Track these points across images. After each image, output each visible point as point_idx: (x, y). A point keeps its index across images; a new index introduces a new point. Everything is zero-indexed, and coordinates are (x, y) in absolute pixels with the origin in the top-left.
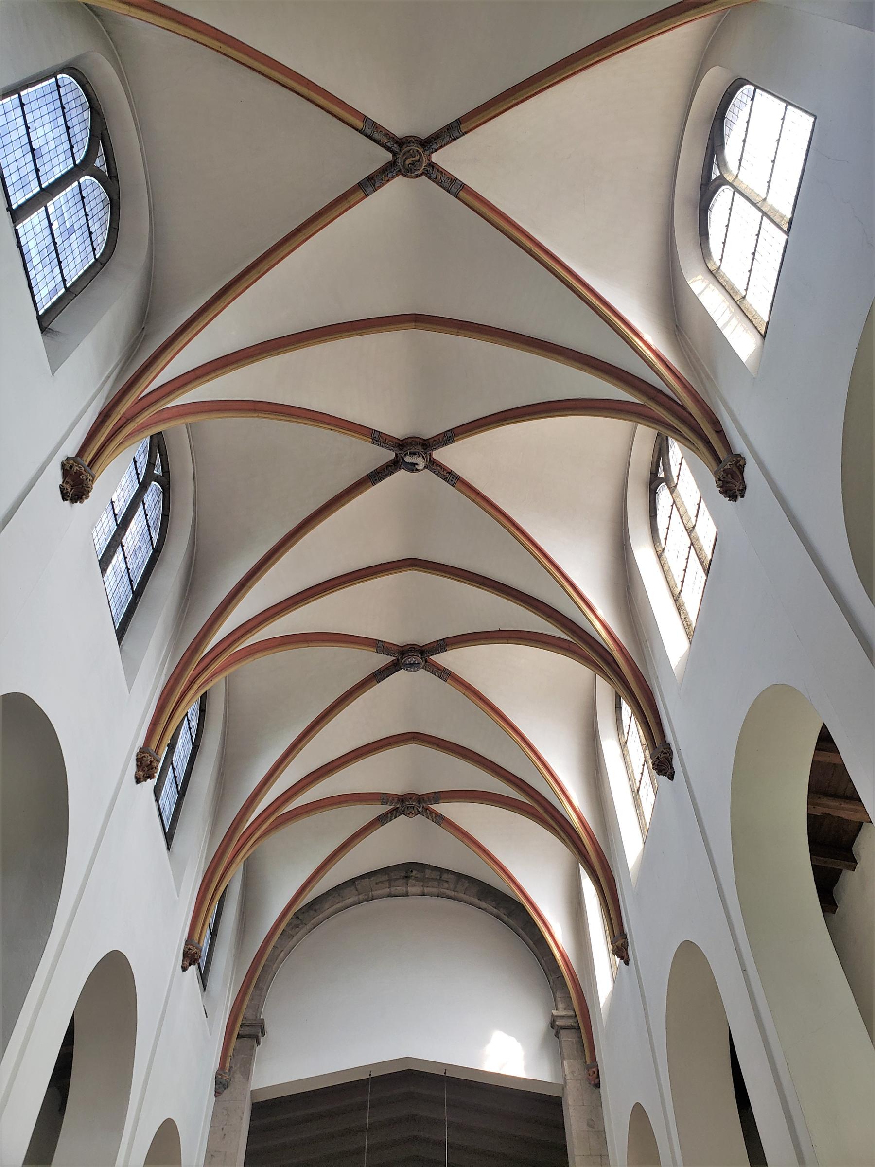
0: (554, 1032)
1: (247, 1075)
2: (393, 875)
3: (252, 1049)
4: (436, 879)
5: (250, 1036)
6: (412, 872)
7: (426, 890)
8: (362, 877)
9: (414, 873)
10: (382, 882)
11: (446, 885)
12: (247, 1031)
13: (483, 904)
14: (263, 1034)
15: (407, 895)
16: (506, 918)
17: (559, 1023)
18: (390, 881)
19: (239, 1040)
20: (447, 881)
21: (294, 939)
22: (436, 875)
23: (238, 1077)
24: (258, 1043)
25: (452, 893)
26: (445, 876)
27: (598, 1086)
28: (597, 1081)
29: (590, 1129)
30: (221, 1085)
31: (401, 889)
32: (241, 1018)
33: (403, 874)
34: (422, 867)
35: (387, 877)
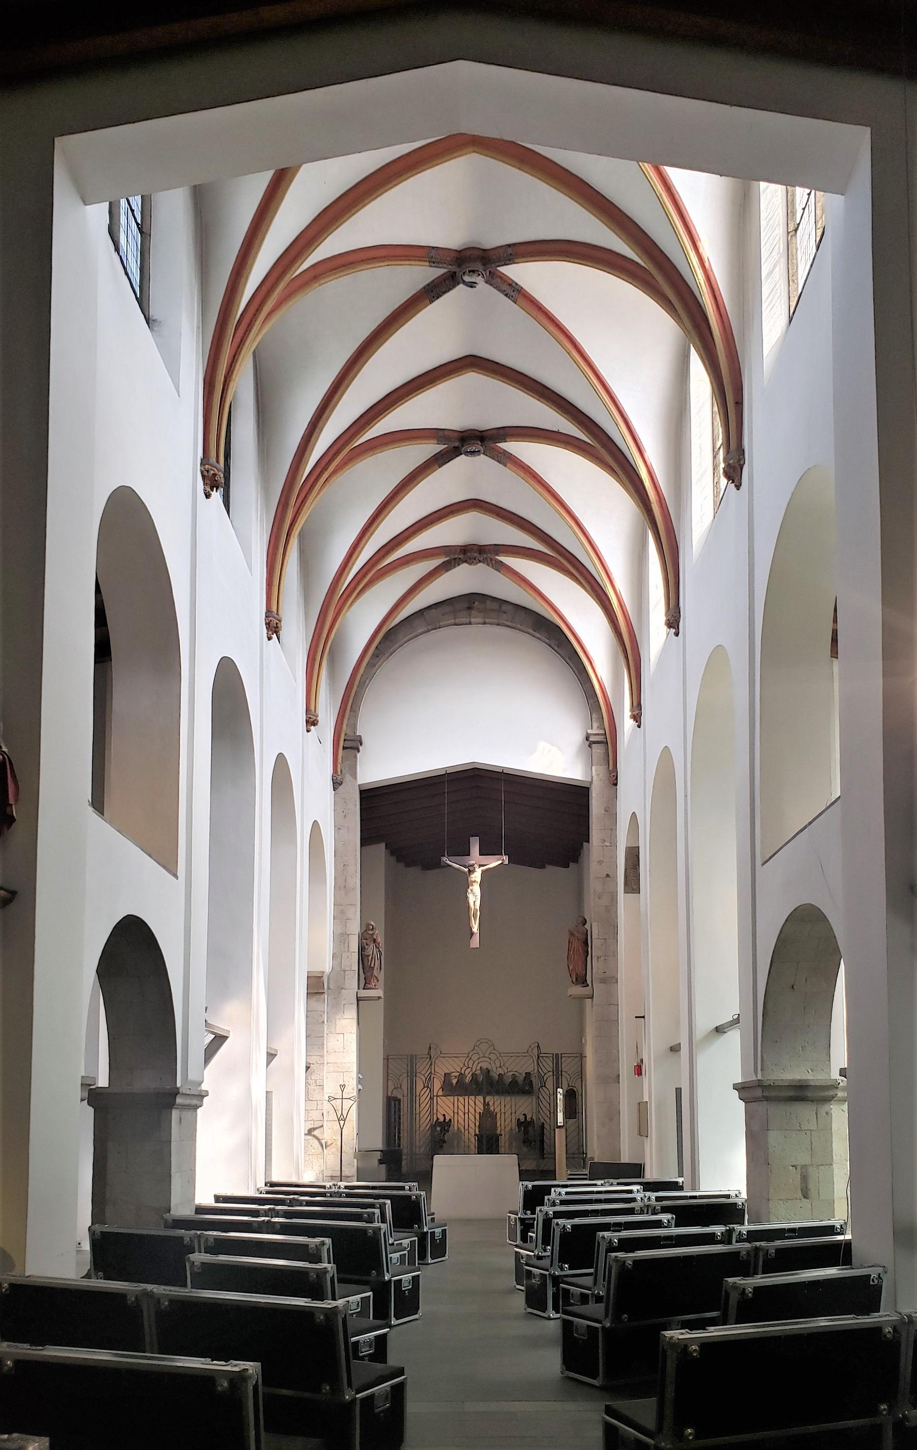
5: (351, 748)
6: (474, 603)
7: (487, 620)
9: (476, 603)
11: (505, 615)
12: (348, 744)
14: (361, 744)
16: (556, 648)
22: (495, 605)
23: (348, 778)
24: (359, 751)
26: (505, 607)
27: (616, 784)
28: (615, 782)
29: (606, 813)
30: (337, 784)
33: (466, 605)
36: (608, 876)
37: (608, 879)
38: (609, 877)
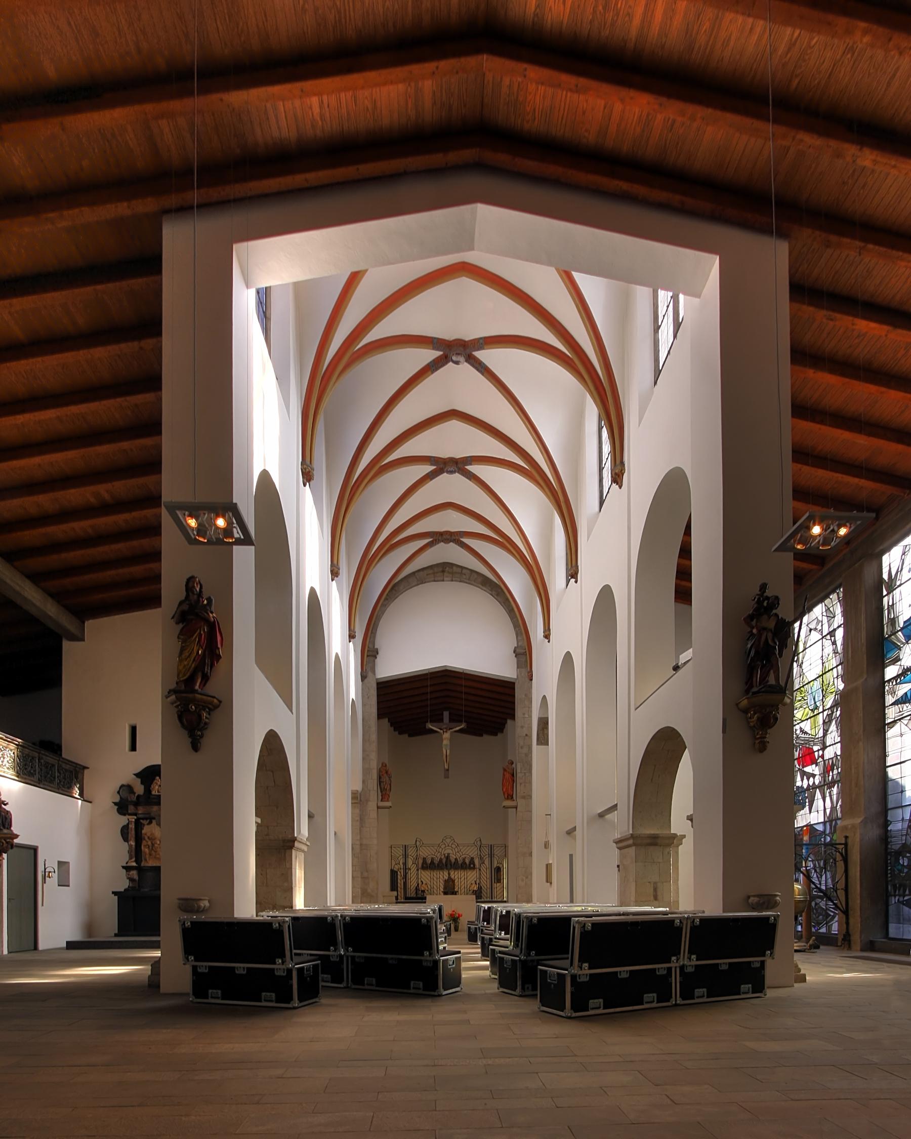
0: (514, 655)
1: (374, 672)
2: (436, 570)
3: (374, 661)
4: (459, 573)
8: (419, 571)
9: (447, 569)
10: (430, 574)
11: (464, 577)
12: (370, 653)
13: (484, 588)
14: (378, 654)
15: (443, 581)
16: (496, 597)
17: (518, 651)
18: (434, 573)
19: (368, 658)
20: (465, 574)
21: (387, 606)
22: (459, 570)
24: (376, 658)
25: (468, 581)
26: (464, 571)
27: (532, 680)
31: (439, 578)
32: (367, 648)
33: (441, 569)
34: (451, 565)
35: (431, 571)
36: (526, 735)
37: (526, 737)
38: (528, 736)
